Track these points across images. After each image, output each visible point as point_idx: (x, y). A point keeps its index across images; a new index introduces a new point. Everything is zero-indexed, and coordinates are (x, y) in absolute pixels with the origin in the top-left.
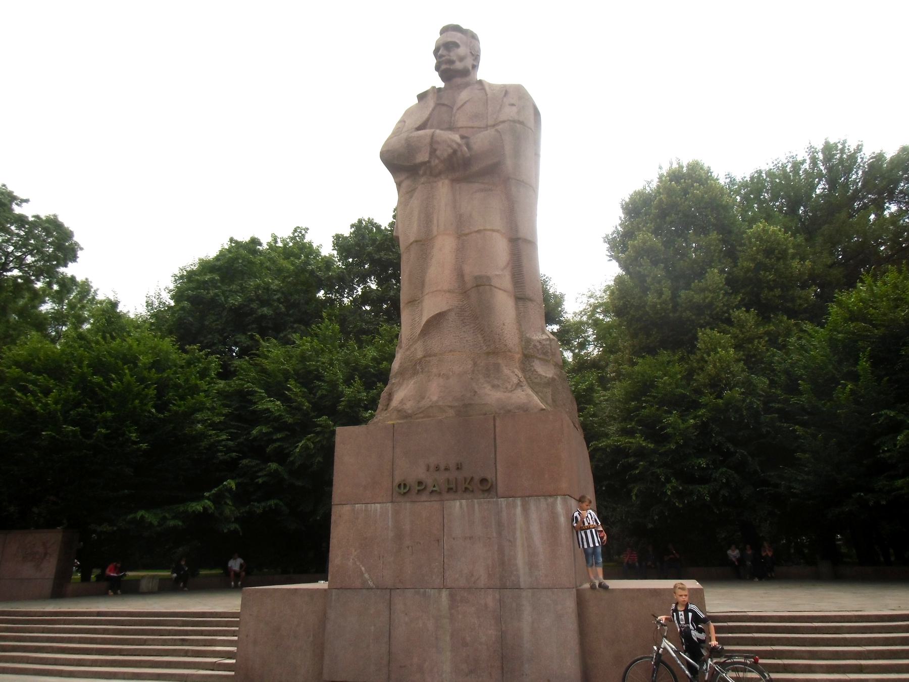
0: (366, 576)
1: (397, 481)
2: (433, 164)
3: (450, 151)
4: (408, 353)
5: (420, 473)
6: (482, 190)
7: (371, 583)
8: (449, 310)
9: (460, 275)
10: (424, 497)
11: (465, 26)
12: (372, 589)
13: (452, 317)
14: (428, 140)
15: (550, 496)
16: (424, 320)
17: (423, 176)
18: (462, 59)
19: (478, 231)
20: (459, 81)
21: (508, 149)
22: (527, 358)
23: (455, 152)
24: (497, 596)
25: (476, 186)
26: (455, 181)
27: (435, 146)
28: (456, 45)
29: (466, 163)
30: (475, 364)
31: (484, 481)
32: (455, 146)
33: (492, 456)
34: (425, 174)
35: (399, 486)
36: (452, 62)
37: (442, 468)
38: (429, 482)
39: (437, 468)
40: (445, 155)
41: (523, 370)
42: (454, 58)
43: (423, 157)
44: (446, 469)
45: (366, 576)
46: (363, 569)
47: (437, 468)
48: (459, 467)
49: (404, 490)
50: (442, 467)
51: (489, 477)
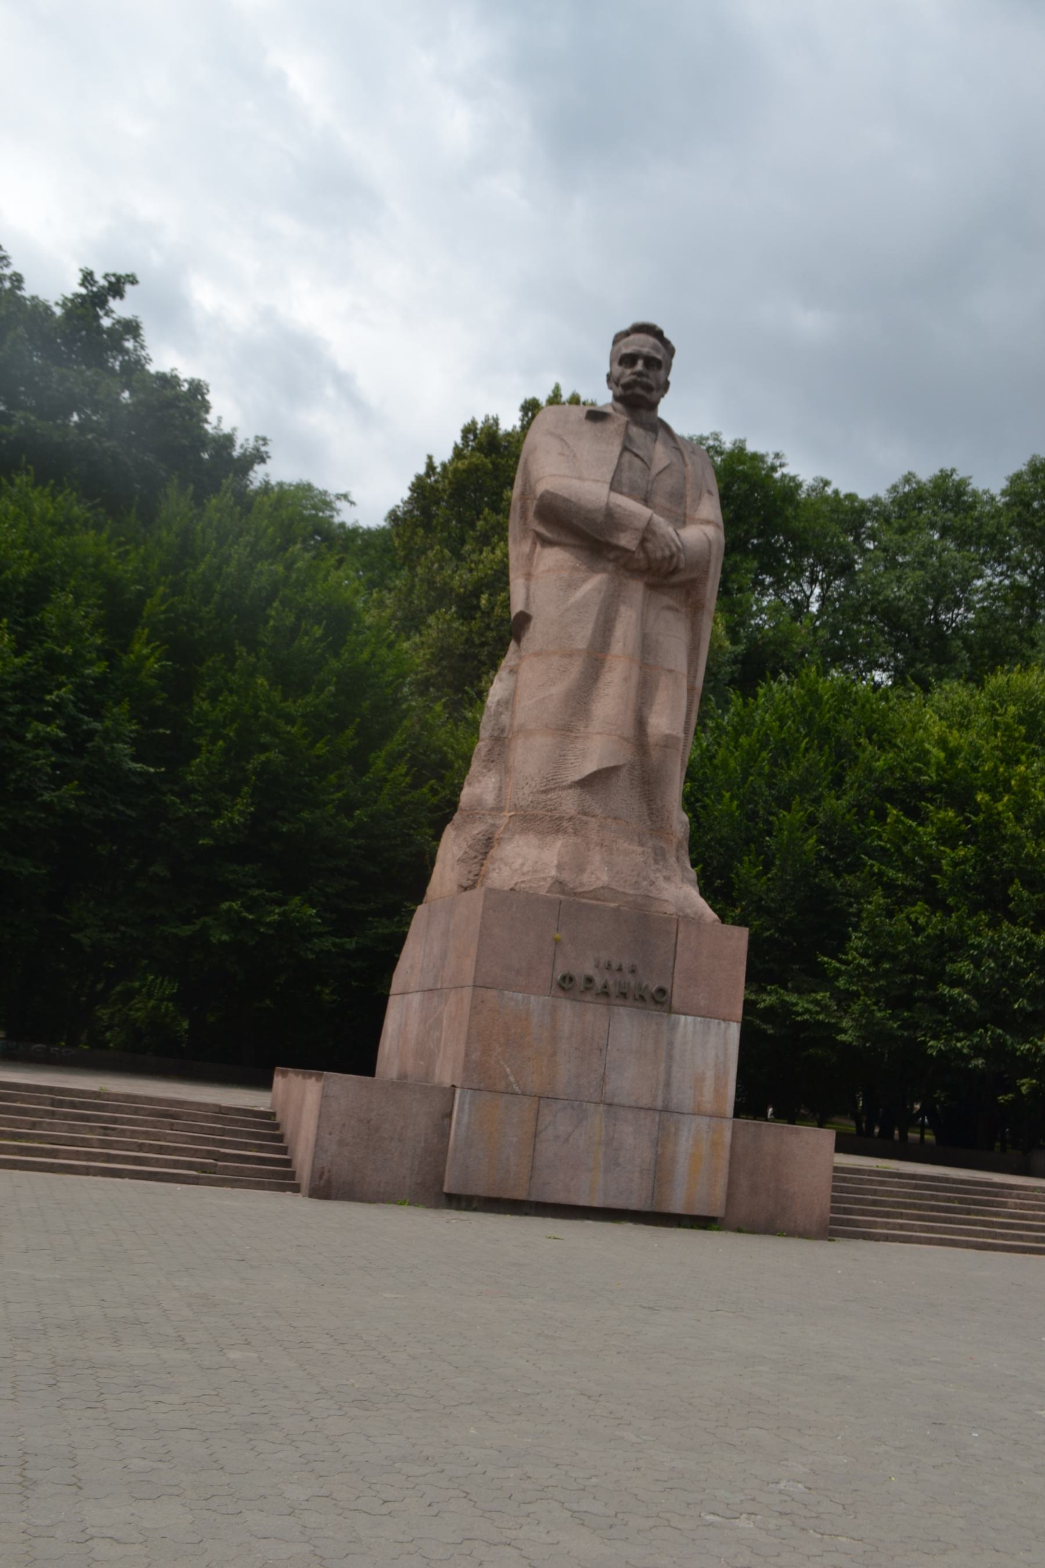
0: (512, 1079)
2: (636, 556)
3: (667, 553)
4: (543, 797)
7: (517, 1089)
8: (624, 765)
10: (589, 997)
11: (667, 335)
12: (516, 1094)
13: (624, 773)
14: (641, 524)
15: (724, 1020)
16: (590, 767)
17: (610, 561)
23: (672, 556)
24: (657, 1119)
26: (651, 587)
27: (650, 536)
31: (662, 991)
32: (674, 549)
33: (671, 964)
34: (615, 560)
35: (564, 978)
37: (615, 966)
38: (599, 981)
39: (609, 966)
40: (659, 554)
42: (653, 383)
43: (627, 540)
44: (620, 969)
45: (512, 1079)
46: (508, 1070)
47: (609, 966)
49: (566, 983)
50: (615, 966)
51: (667, 987)
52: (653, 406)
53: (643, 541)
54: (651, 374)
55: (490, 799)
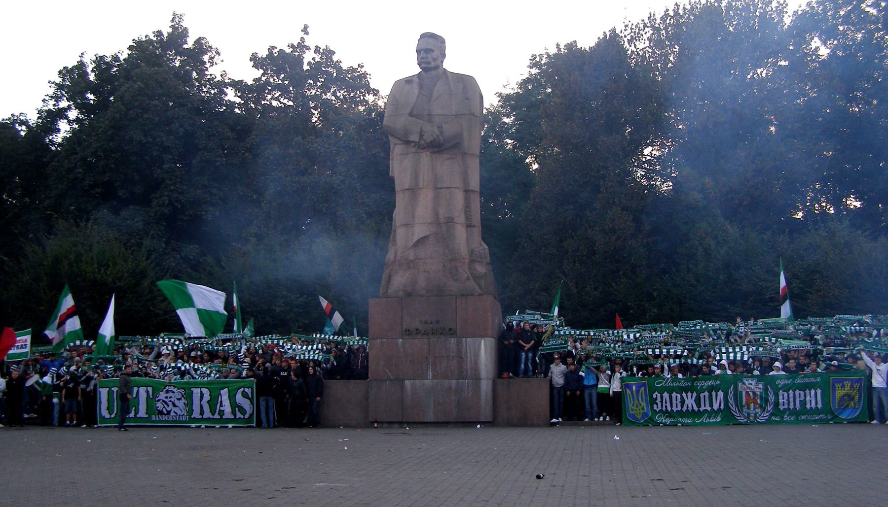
1: (405, 327)
5: (416, 324)
6: (448, 159)
9: (436, 213)
16: (416, 239)
18: (435, 60)
19: (448, 188)
20: (433, 73)
21: (465, 133)
22: (472, 261)
25: (446, 156)
28: (432, 51)
29: (440, 145)
30: (444, 266)
36: (429, 63)
39: (426, 322)
40: (429, 140)
41: (470, 269)
42: (430, 60)
48: (438, 322)
52: (438, 67)
53: (421, 136)
54: (429, 56)
55: (392, 258)
